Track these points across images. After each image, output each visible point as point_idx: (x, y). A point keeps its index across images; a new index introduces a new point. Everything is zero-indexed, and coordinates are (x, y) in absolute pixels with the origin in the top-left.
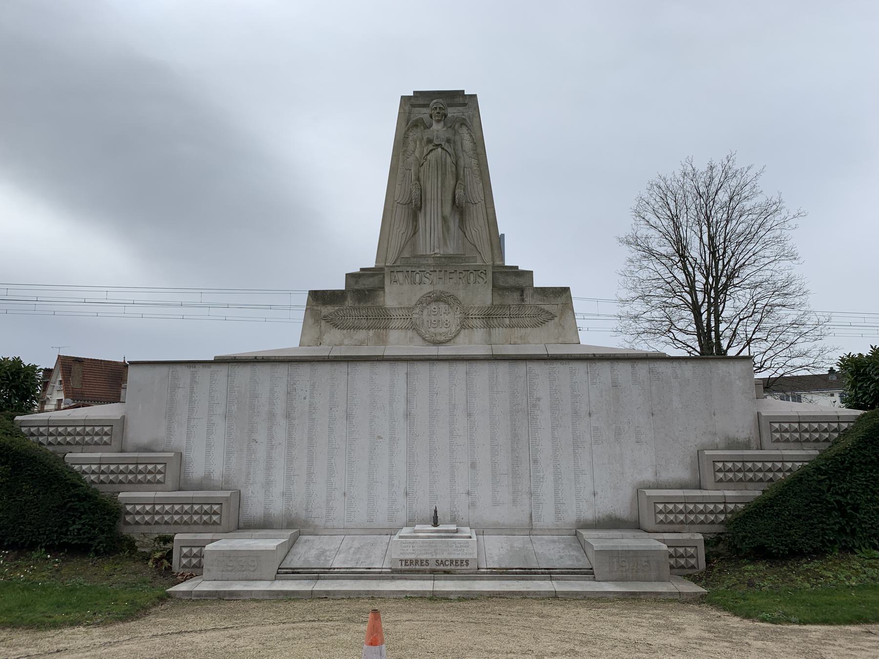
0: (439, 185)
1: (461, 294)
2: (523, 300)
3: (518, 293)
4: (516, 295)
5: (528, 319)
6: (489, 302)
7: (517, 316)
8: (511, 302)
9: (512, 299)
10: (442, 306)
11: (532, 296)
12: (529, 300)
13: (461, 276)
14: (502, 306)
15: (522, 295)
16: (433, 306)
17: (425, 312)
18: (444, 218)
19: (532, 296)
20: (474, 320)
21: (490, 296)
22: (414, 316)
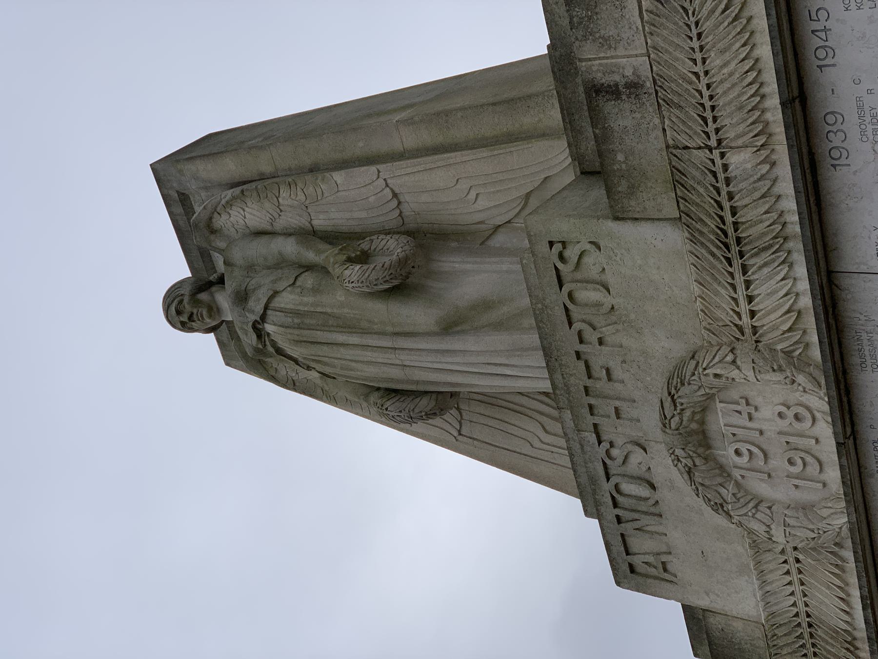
0: (354, 339)
1: (663, 346)
2: (634, 87)
3: (609, 107)
4: (622, 117)
5: (715, 61)
6: (670, 238)
7: (708, 114)
8: (656, 141)
9: (640, 136)
10: (722, 419)
11: (606, 42)
12: (628, 59)
13: (591, 336)
14: (678, 180)
15: (614, 92)
16: (726, 453)
17: (760, 487)
18: (450, 327)
19: (606, 42)
20: (759, 305)
21: (646, 230)
22: (778, 535)
